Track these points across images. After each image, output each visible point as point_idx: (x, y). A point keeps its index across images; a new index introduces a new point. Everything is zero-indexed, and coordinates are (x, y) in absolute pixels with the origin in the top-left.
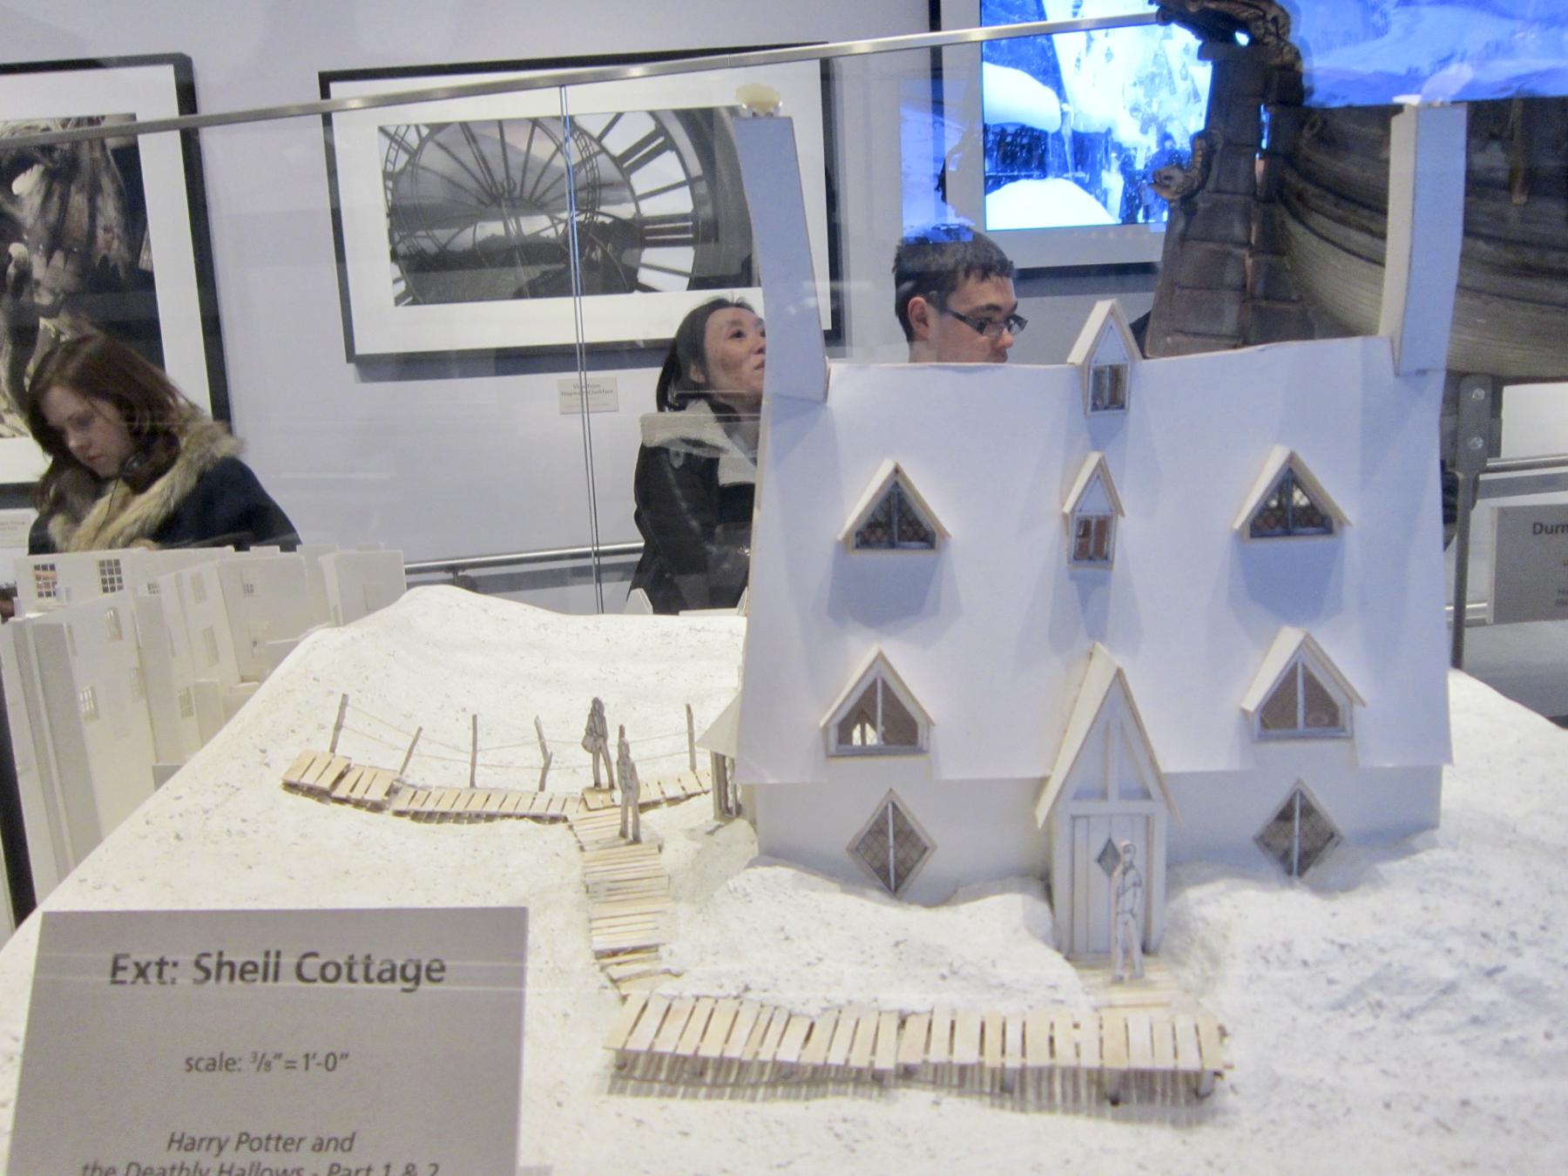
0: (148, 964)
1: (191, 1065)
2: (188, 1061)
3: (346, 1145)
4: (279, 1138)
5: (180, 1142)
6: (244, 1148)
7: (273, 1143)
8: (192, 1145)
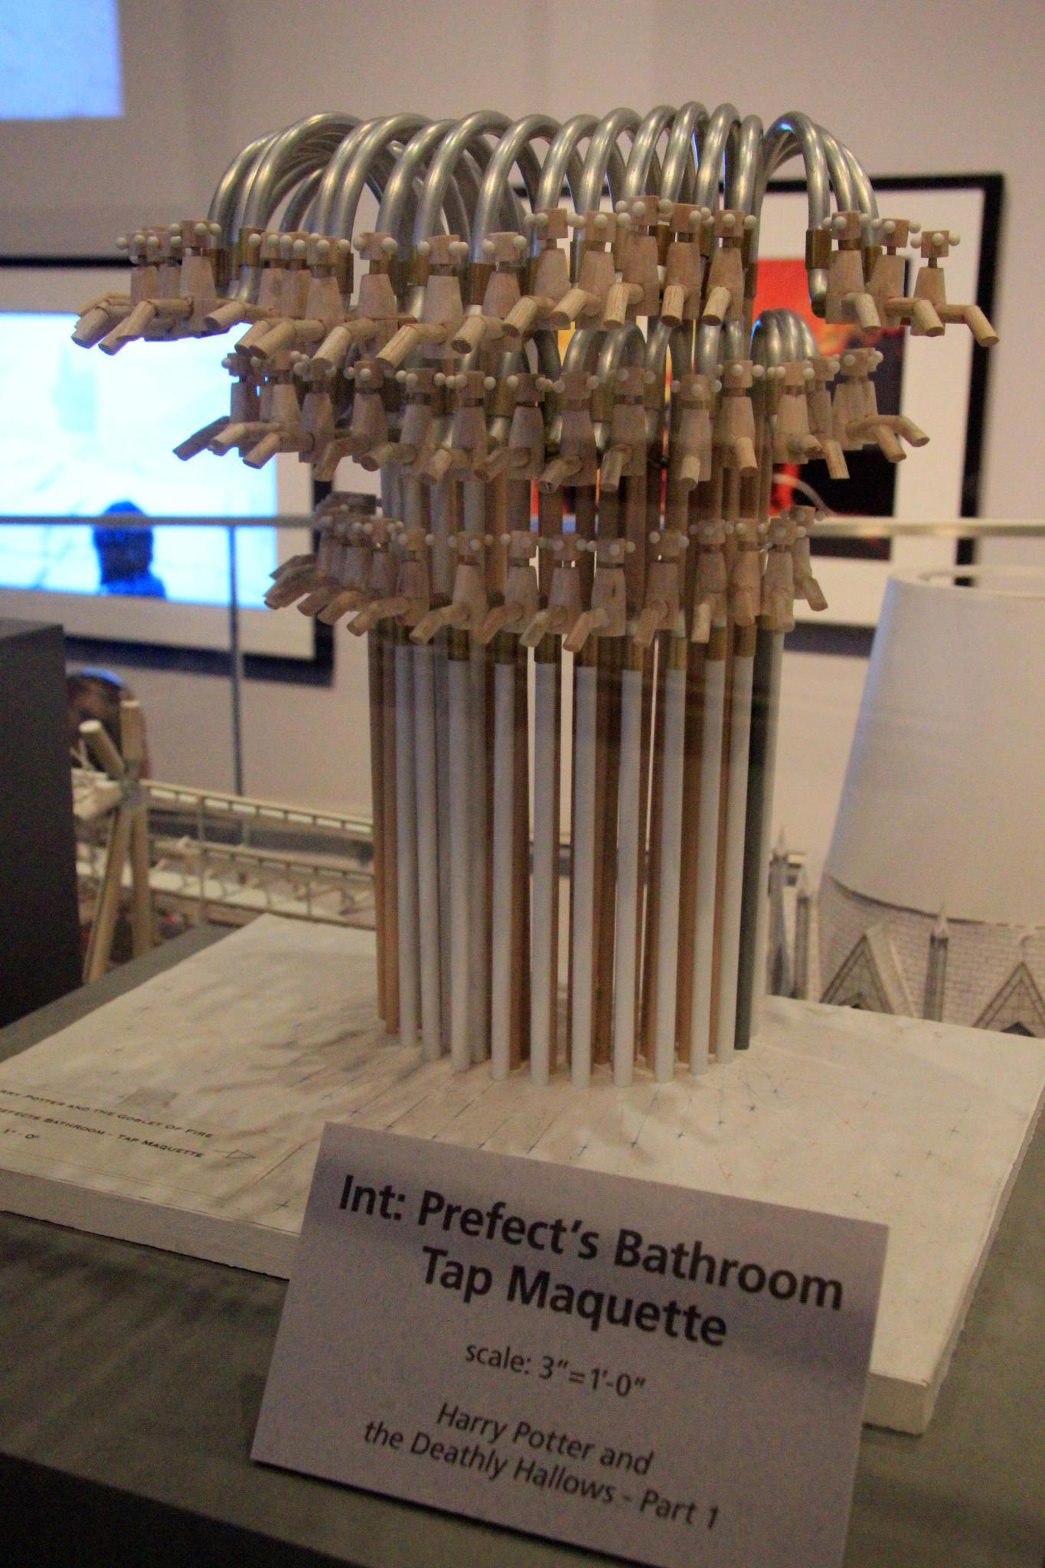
3: (642, 1465)
4: (564, 1439)
6: (523, 1441)
7: (555, 1443)
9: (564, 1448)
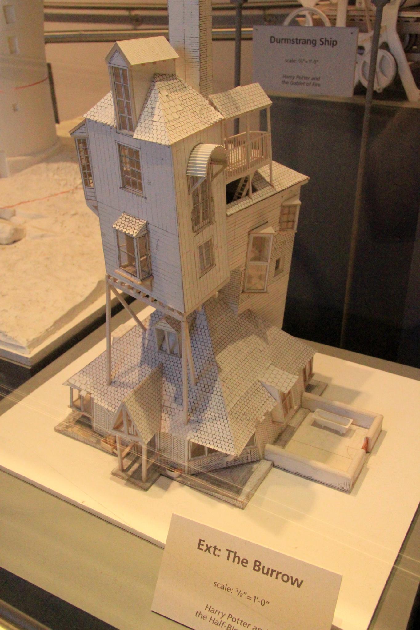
0: (211, 547)
1: (216, 584)
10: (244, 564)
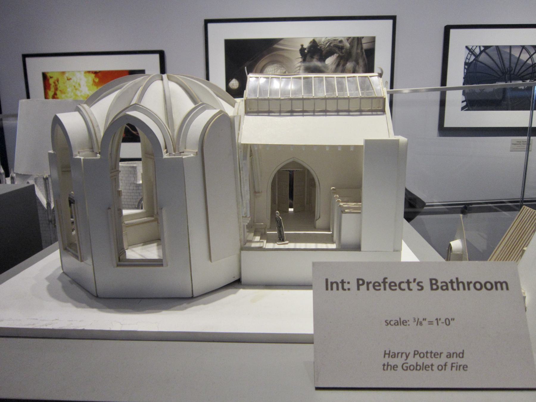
1: (388, 323)
2: (386, 321)
3: (461, 355)
4: (431, 353)
5: (389, 354)
6: (417, 356)
7: (429, 355)
8: (395, 356)
9: (433, 354)
10: (393, 288)
